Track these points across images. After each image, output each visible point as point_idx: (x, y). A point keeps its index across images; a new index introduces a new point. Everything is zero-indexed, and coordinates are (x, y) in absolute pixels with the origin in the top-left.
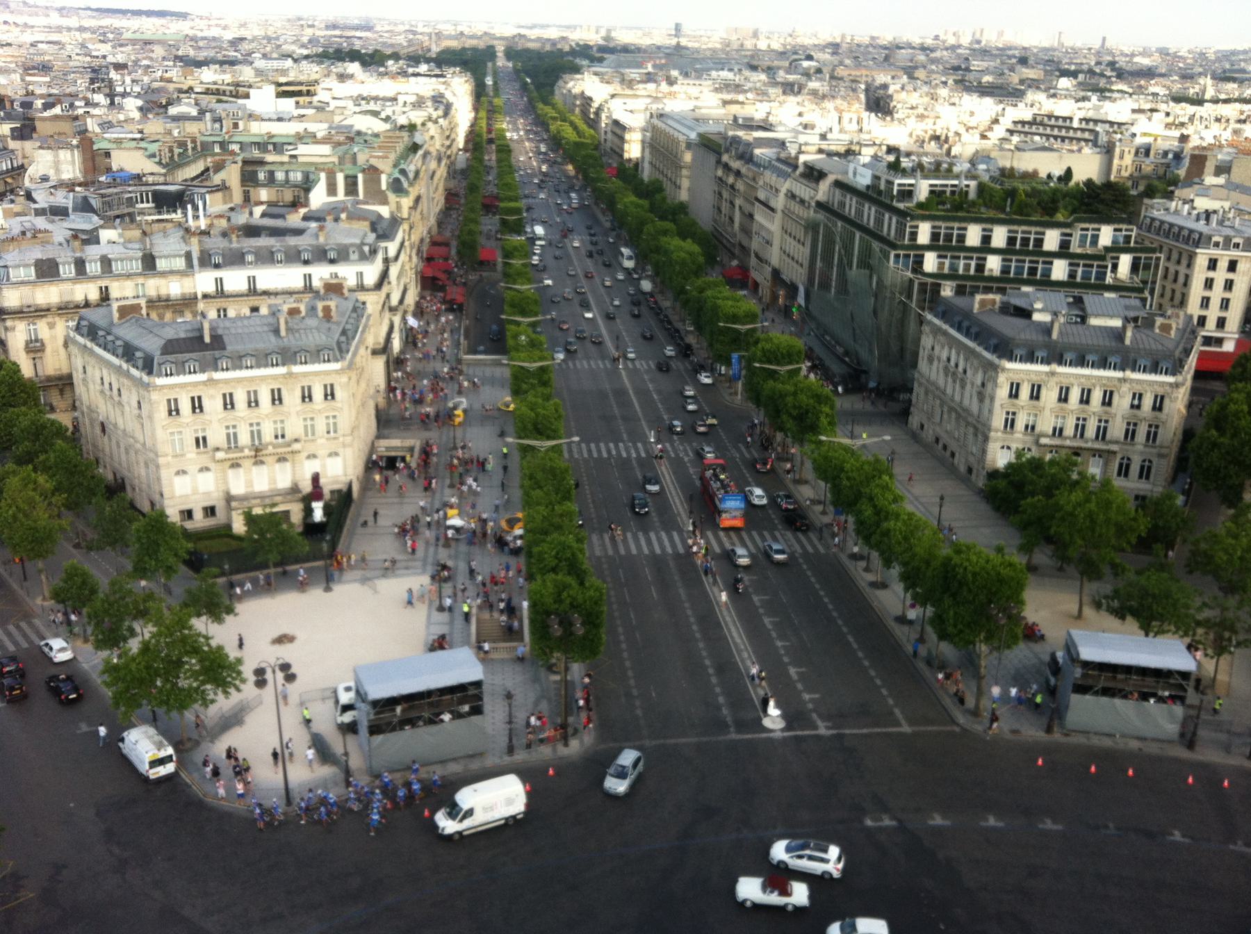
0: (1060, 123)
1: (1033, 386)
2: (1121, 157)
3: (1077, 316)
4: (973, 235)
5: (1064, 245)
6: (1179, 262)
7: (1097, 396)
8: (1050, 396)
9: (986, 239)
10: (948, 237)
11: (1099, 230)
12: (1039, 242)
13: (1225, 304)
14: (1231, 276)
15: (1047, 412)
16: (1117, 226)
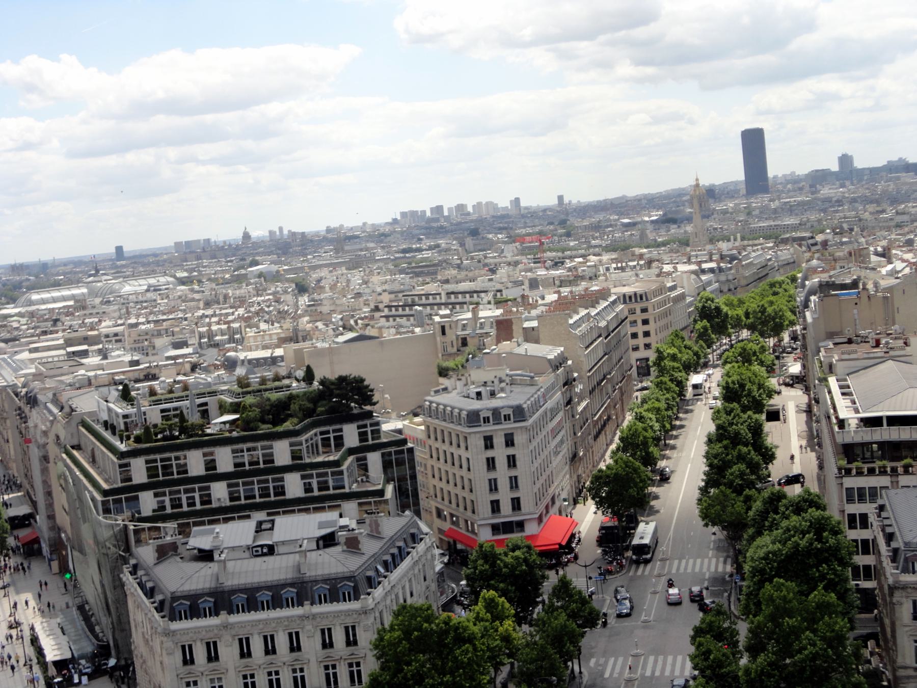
0: (431, 300)
1: (208, 644)
2: (444, 333)
3: (262, 546)
4: (195, 462)
5: (296, 456)
6: (459, 446)
7: (282, 643)
8: (228, 652)
9: (211, 465)
10: (167, 469)
11: (341, 430)
12: (269, 459)
13: (514, 483)
14: (511, 451)
15: (232, 673)
16: (361, 423)
